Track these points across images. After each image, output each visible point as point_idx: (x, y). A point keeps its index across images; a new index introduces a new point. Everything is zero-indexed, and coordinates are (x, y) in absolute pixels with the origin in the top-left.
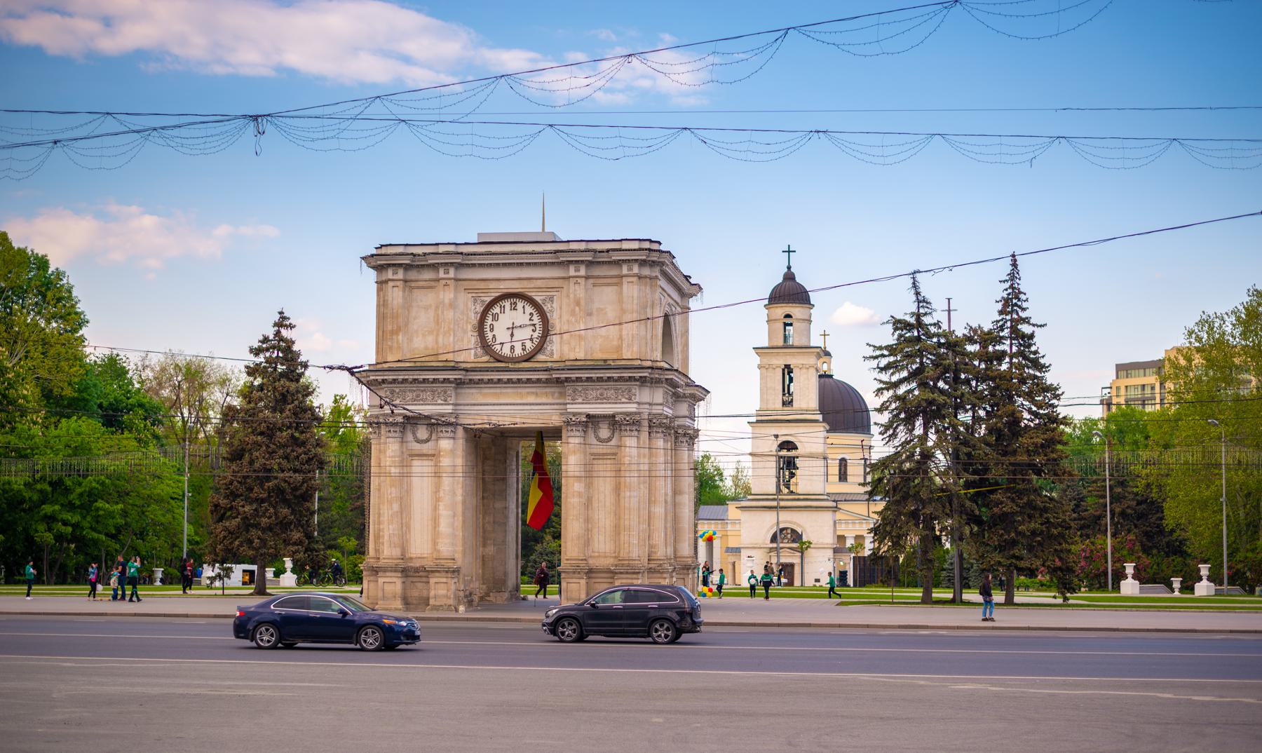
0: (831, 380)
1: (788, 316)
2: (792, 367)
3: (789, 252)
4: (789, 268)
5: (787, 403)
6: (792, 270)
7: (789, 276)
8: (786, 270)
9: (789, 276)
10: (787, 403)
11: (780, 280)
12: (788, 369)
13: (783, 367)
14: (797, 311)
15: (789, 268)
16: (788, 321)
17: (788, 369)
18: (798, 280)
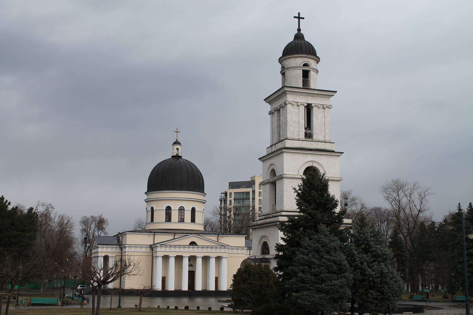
0: (180, 159)
1: (305, 65)
2: (313, 105)
3: (299, 18)
4: (299, 30)
5: (309, 136)
6: (302, 32)
7: (299, 36)
8: (297, 32)
9: (299, 36)
10: (309, 136)
11: (292, 39)
12: (309, 108)
13: (306, 105)
14: (312, 63)
15: (299, 30)
16: (306, 68)
17: (309, 108)
18: (307, 39)
